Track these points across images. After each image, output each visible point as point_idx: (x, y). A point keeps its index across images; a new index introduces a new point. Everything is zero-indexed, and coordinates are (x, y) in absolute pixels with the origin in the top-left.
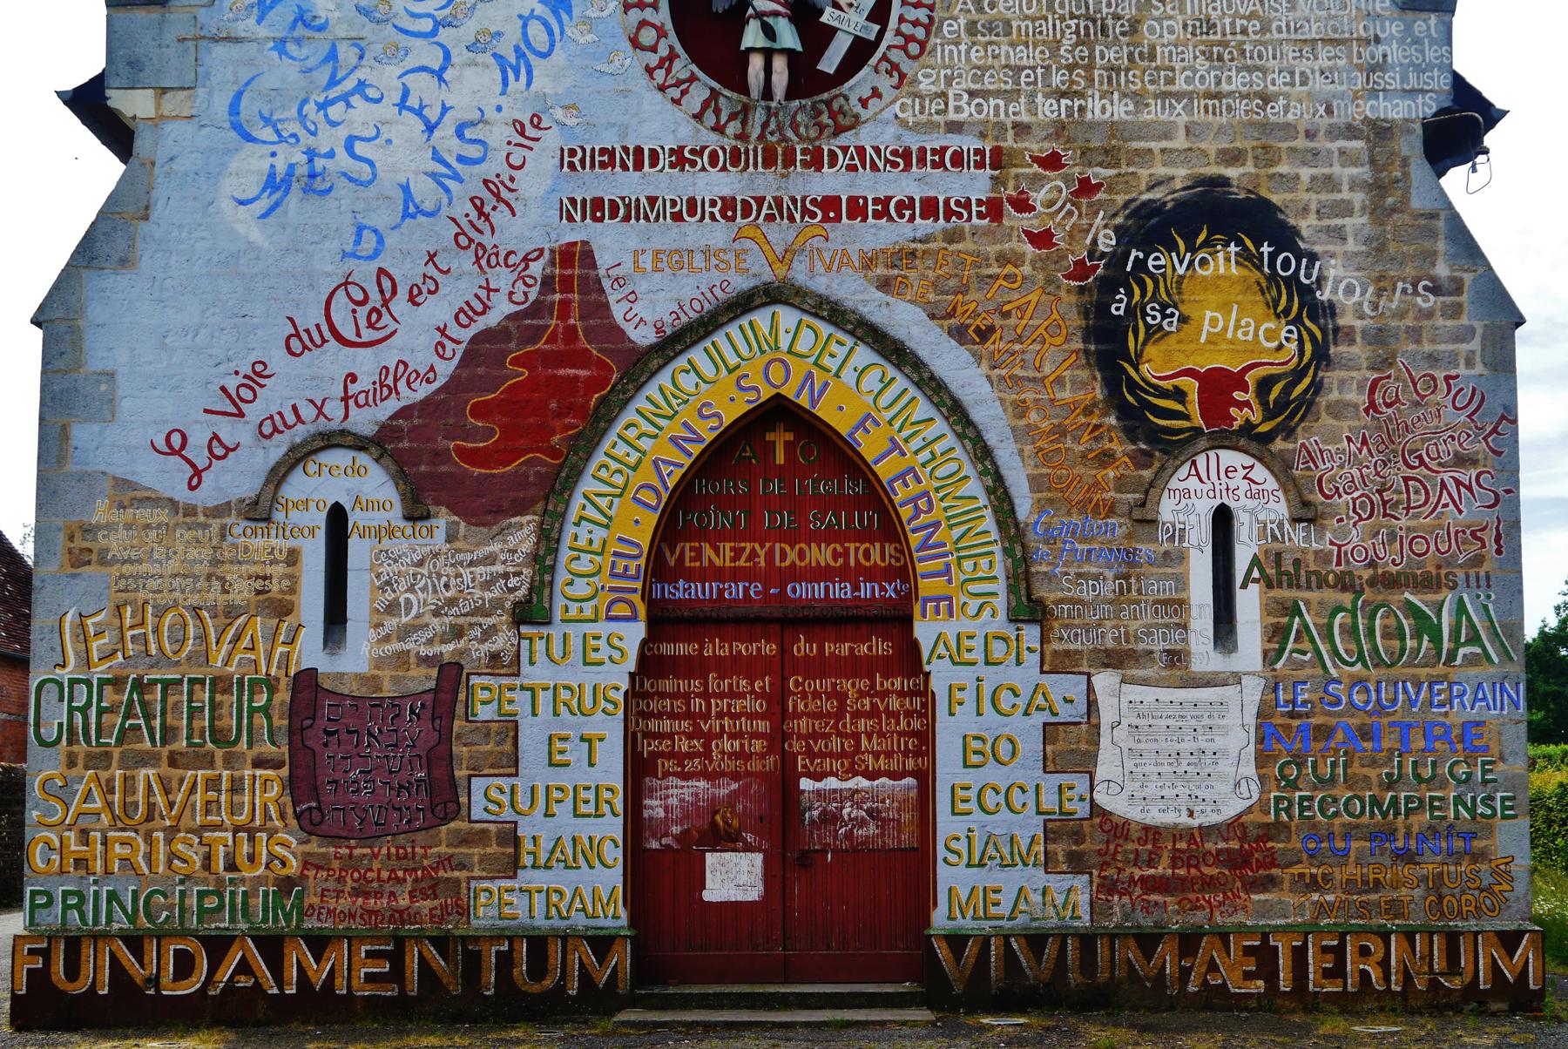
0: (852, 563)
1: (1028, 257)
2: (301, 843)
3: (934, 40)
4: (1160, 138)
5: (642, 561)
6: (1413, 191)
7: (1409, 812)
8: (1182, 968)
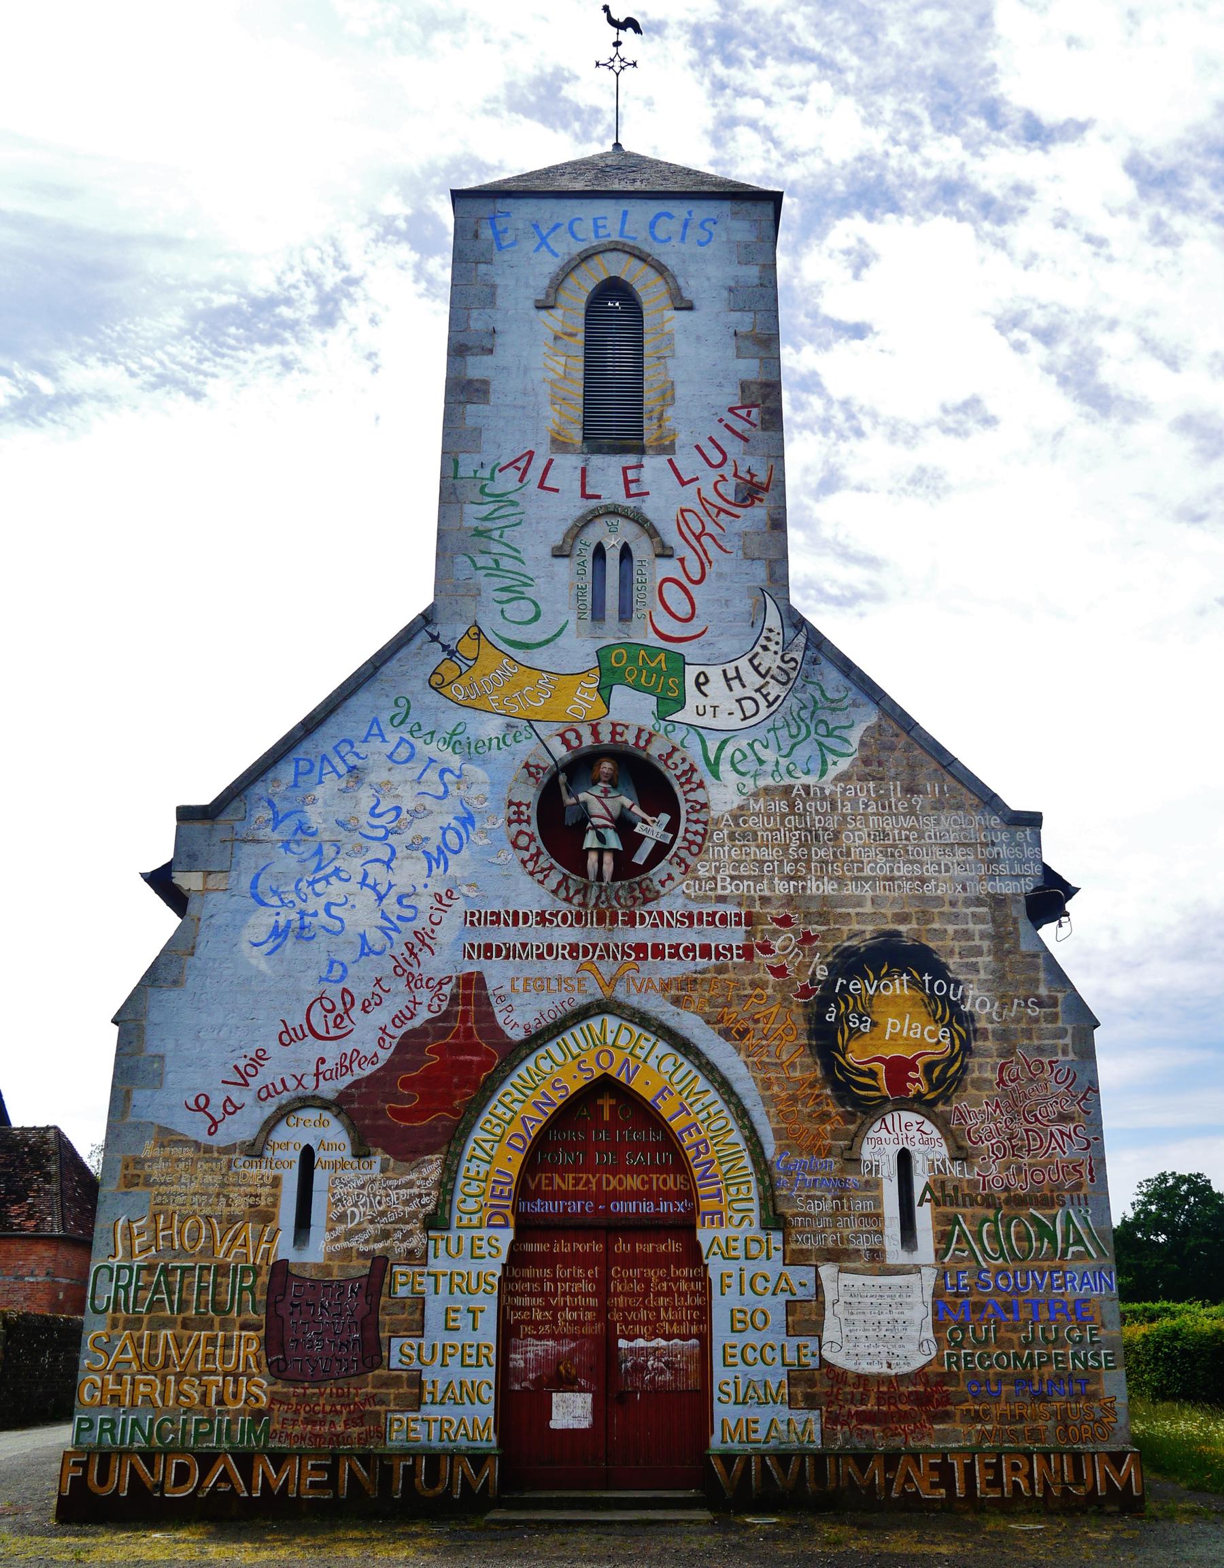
0: (655, 1188)
1: (771, 984)
2: (270, 1384)
3: (707, 844)
4: (854, 906)
5: (513, 1187)
6: (1021, 940)
7: (1041, 1364)
8: (887, 1480)
